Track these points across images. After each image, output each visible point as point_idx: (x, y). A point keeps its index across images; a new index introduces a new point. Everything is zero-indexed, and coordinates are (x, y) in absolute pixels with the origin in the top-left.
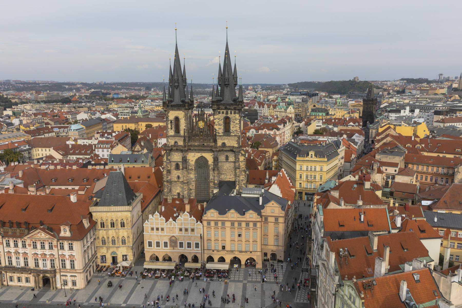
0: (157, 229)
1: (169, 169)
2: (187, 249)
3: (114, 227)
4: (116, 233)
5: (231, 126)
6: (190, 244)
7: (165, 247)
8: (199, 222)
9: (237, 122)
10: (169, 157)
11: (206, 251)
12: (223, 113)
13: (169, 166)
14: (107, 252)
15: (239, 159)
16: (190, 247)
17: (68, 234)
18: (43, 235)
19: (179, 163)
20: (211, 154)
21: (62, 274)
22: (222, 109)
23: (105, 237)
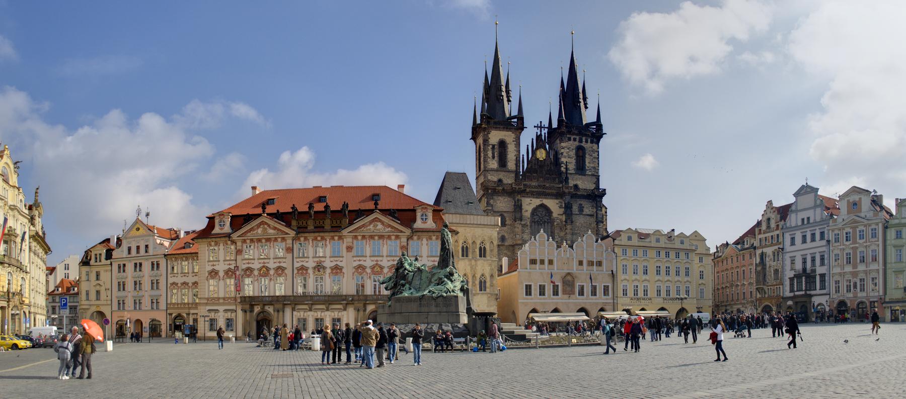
0: (542, 262)
4: (471, 268)
5: (587, 161)
10: (491, 202)
12: (575, 140)
16: (595, 295)
19: (505, 215)
20: (557, 201)
22: (573, 134)
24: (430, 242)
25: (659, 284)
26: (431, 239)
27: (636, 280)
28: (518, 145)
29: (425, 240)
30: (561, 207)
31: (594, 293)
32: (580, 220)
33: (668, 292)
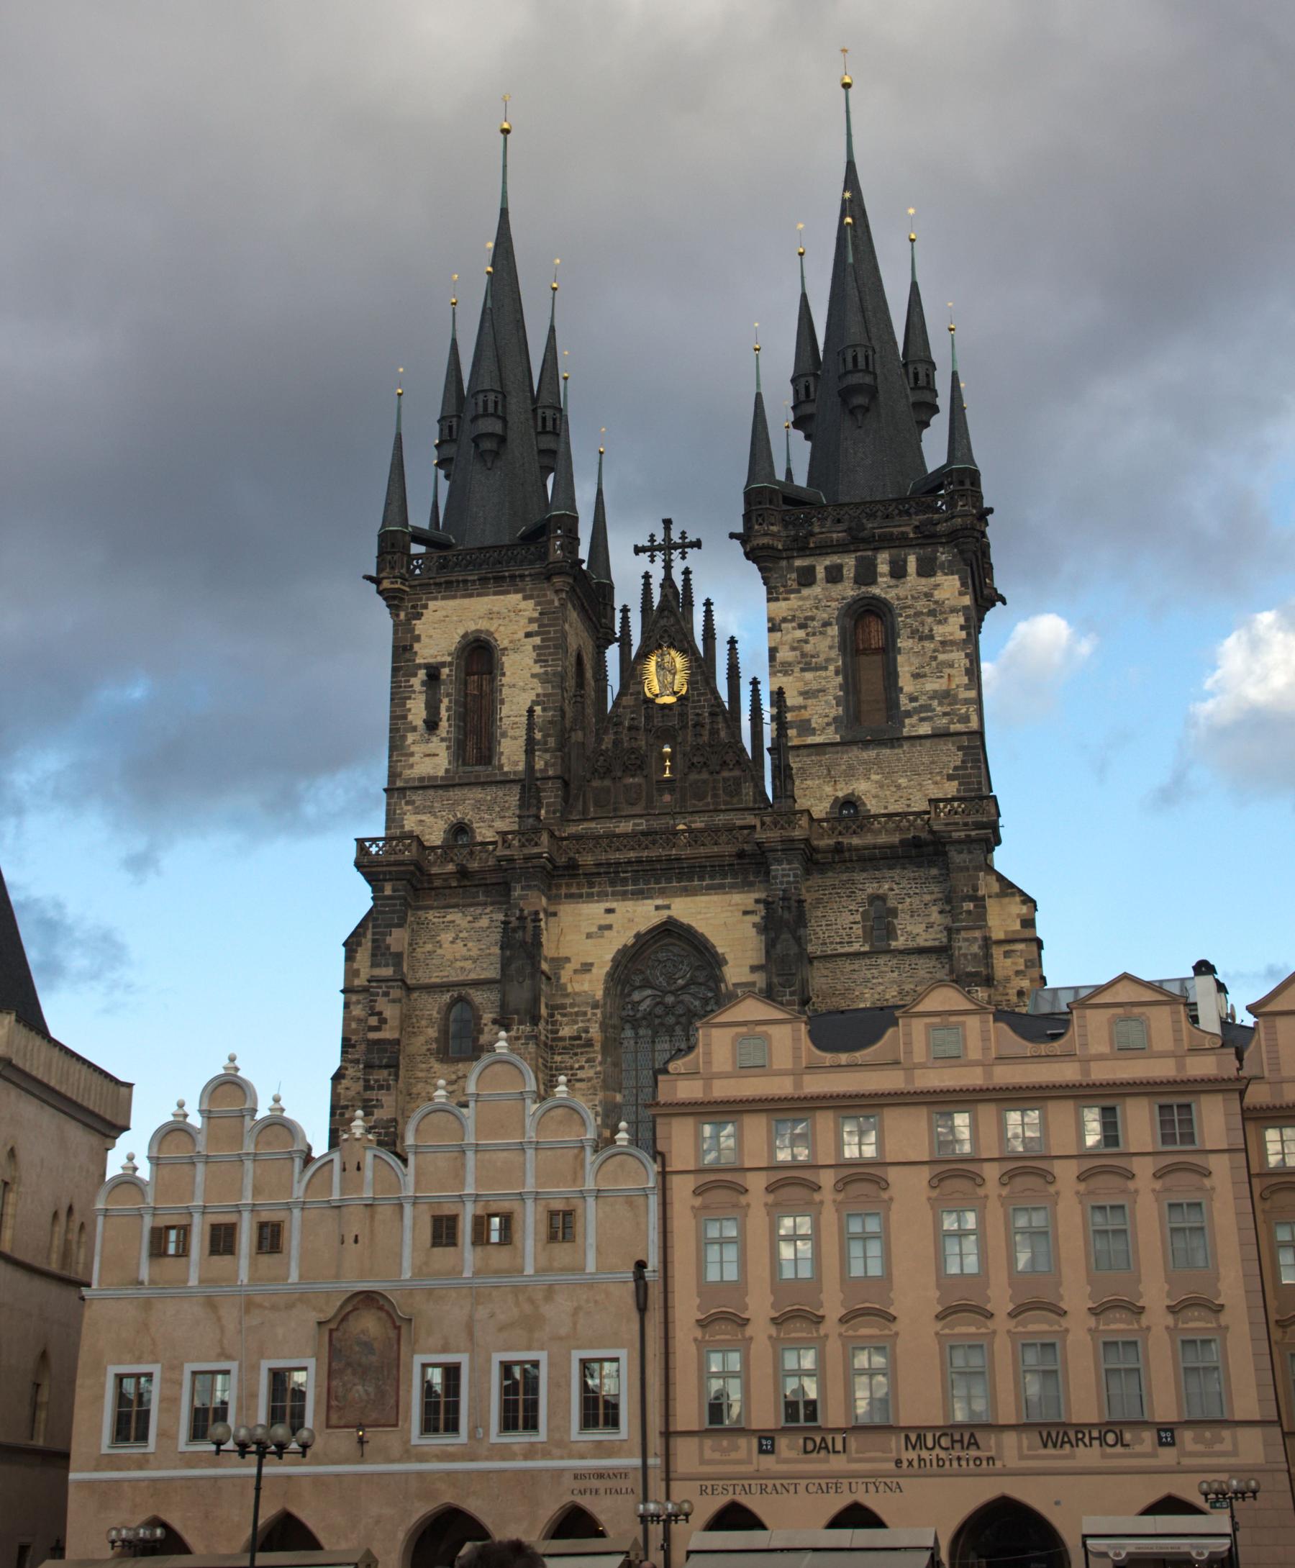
0: (222, 1239)
1: (387, 1034)
2: (495, 1436)
5: (905, 668)
6: (532, 1384)
8: (622, 1137)
9: (953, 628)
10: (397, 939)
11: (687, 1455)
12: (834, 575)
13: (390, 1011)
15: (979, 901)
16: (531, 1424)
19: (478, 997)
20: (746, 899)
22: (825, 549)
31: (519, 1408)
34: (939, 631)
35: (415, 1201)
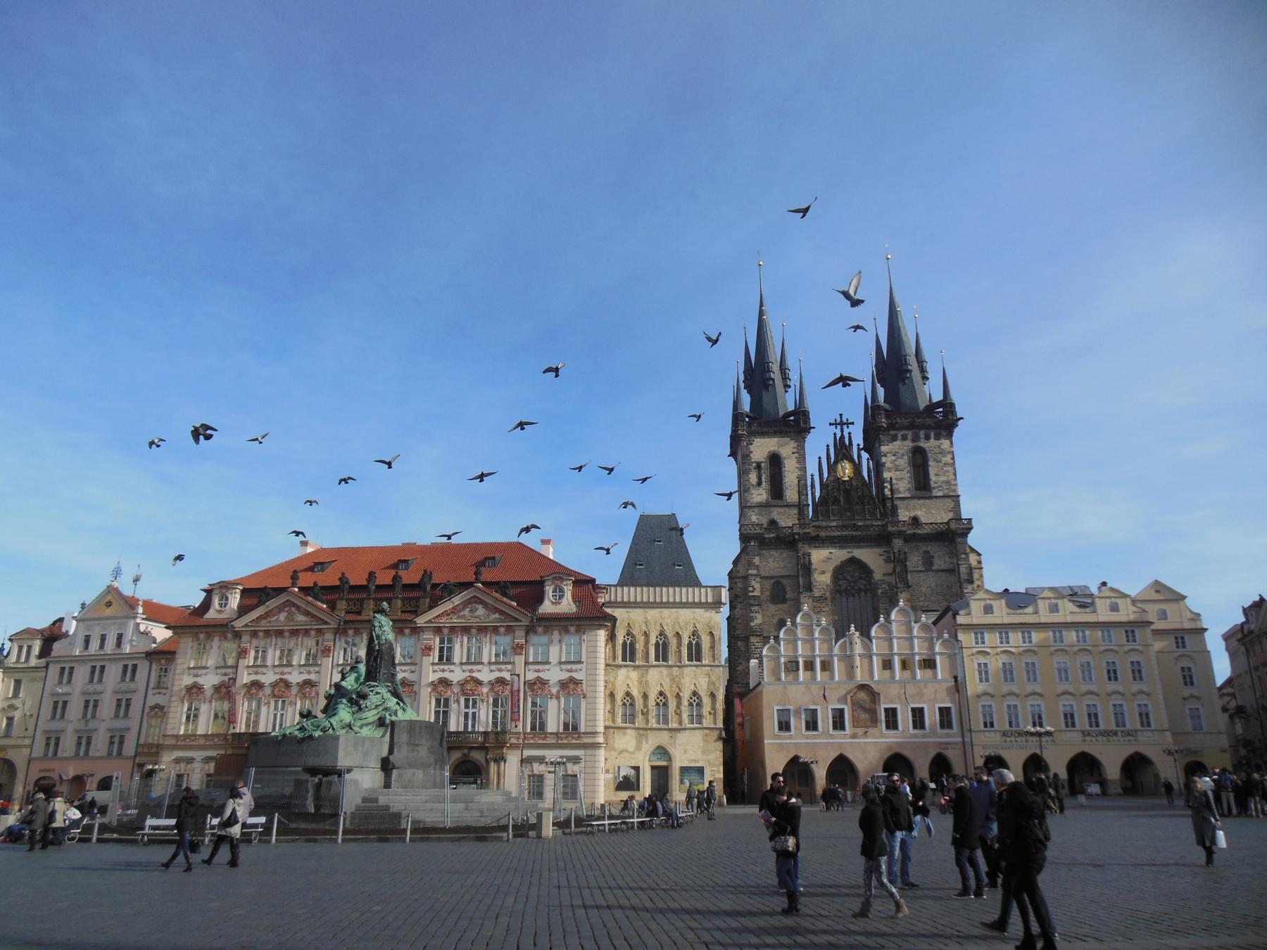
0: (810, 666)
3: (665, 659)
4: (673, 680)
5: (932, 471)
7: (835, 728)
12: (904, 438)
13: (757, 586)
14: (638, 748)
15: (967, 554)
17: (567, 605)
18: (481, 611)
19: (784, 581)
20: (881, 550)
21: (527, 753)
22: (901, 429)
23: (635, 693)
24: (567, 638)
25: (1068, 701)
26: (567, 631)
27: (1011, 694)
28: (802, 458)
29: (556, 633)
30: (887, 561)
32: (925, 583)
33: (1093, 717)
34: (944, 459)
35: (877, 655)
